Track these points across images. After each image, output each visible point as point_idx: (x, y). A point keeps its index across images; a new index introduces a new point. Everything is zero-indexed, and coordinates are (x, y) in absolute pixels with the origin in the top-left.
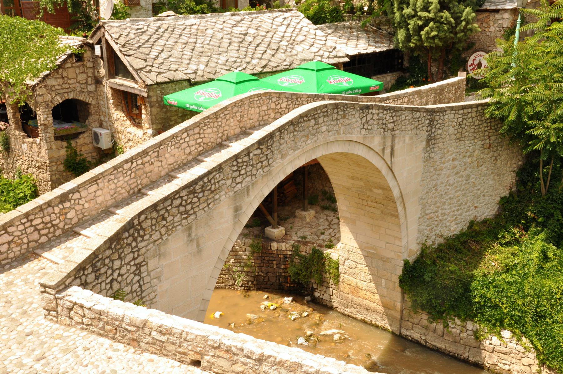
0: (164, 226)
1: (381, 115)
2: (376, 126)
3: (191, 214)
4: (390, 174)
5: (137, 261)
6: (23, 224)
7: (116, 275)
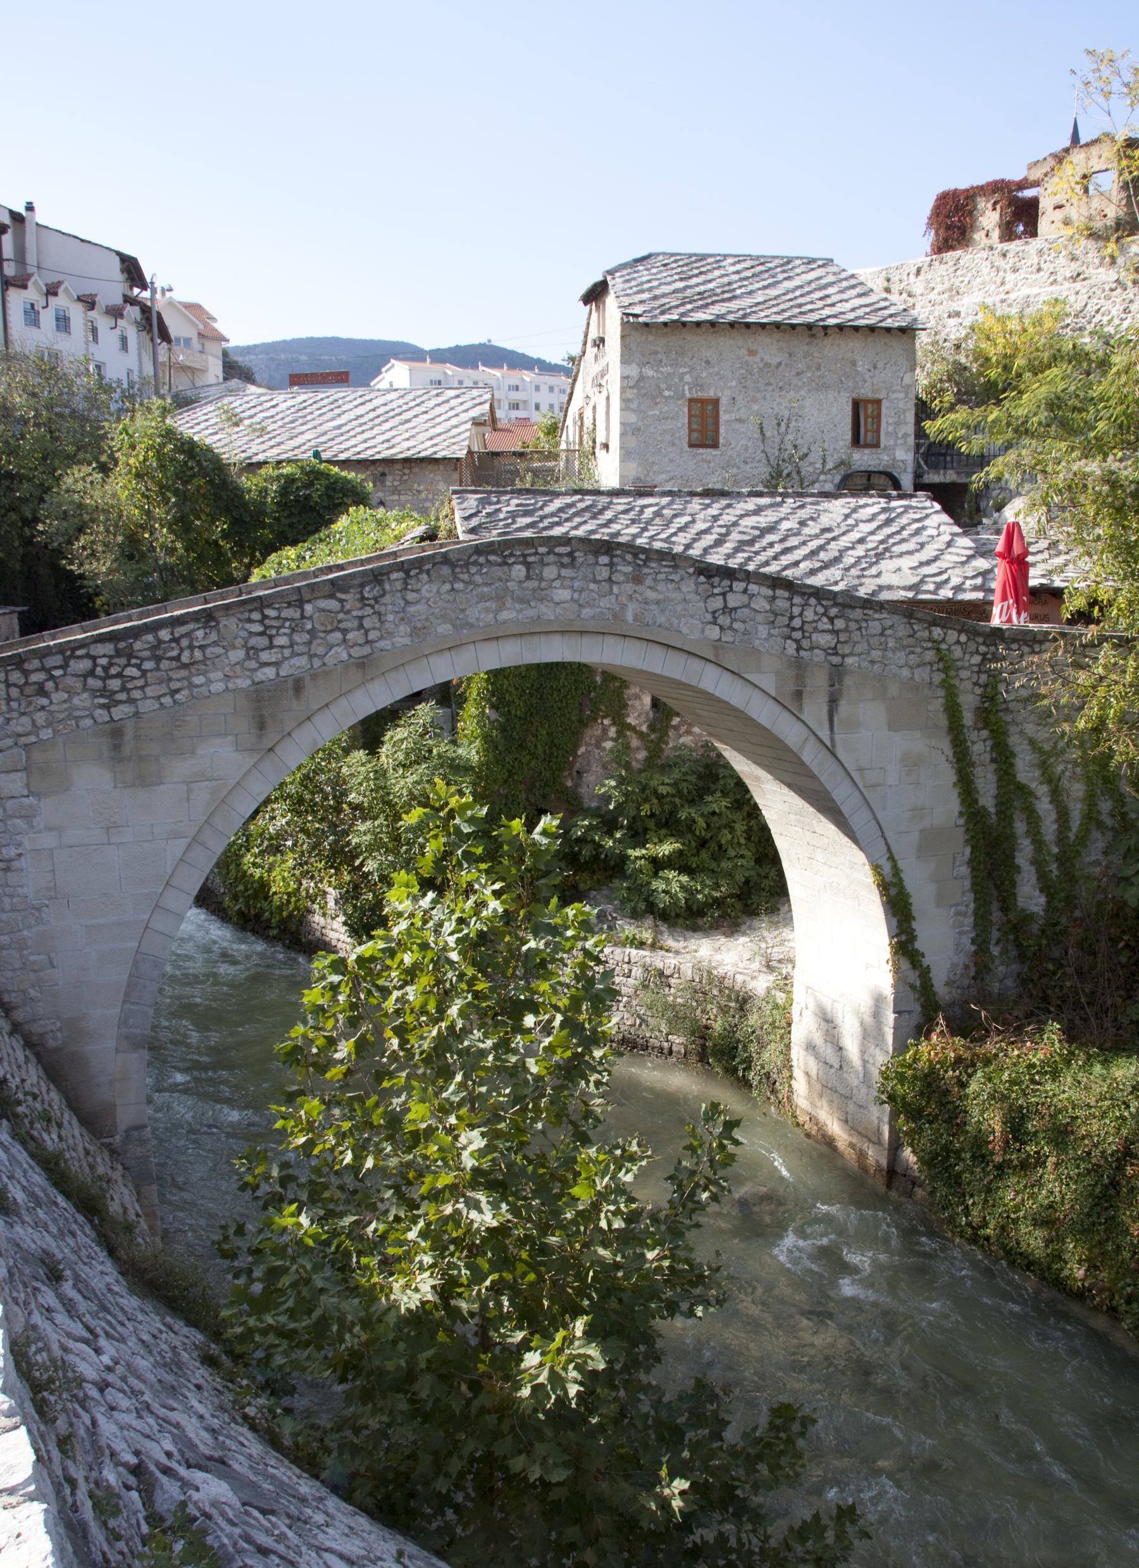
0: (43, 708)
1: (782, 604)
2: (763, 631)
3: (121, 702)
4: (831, 765)
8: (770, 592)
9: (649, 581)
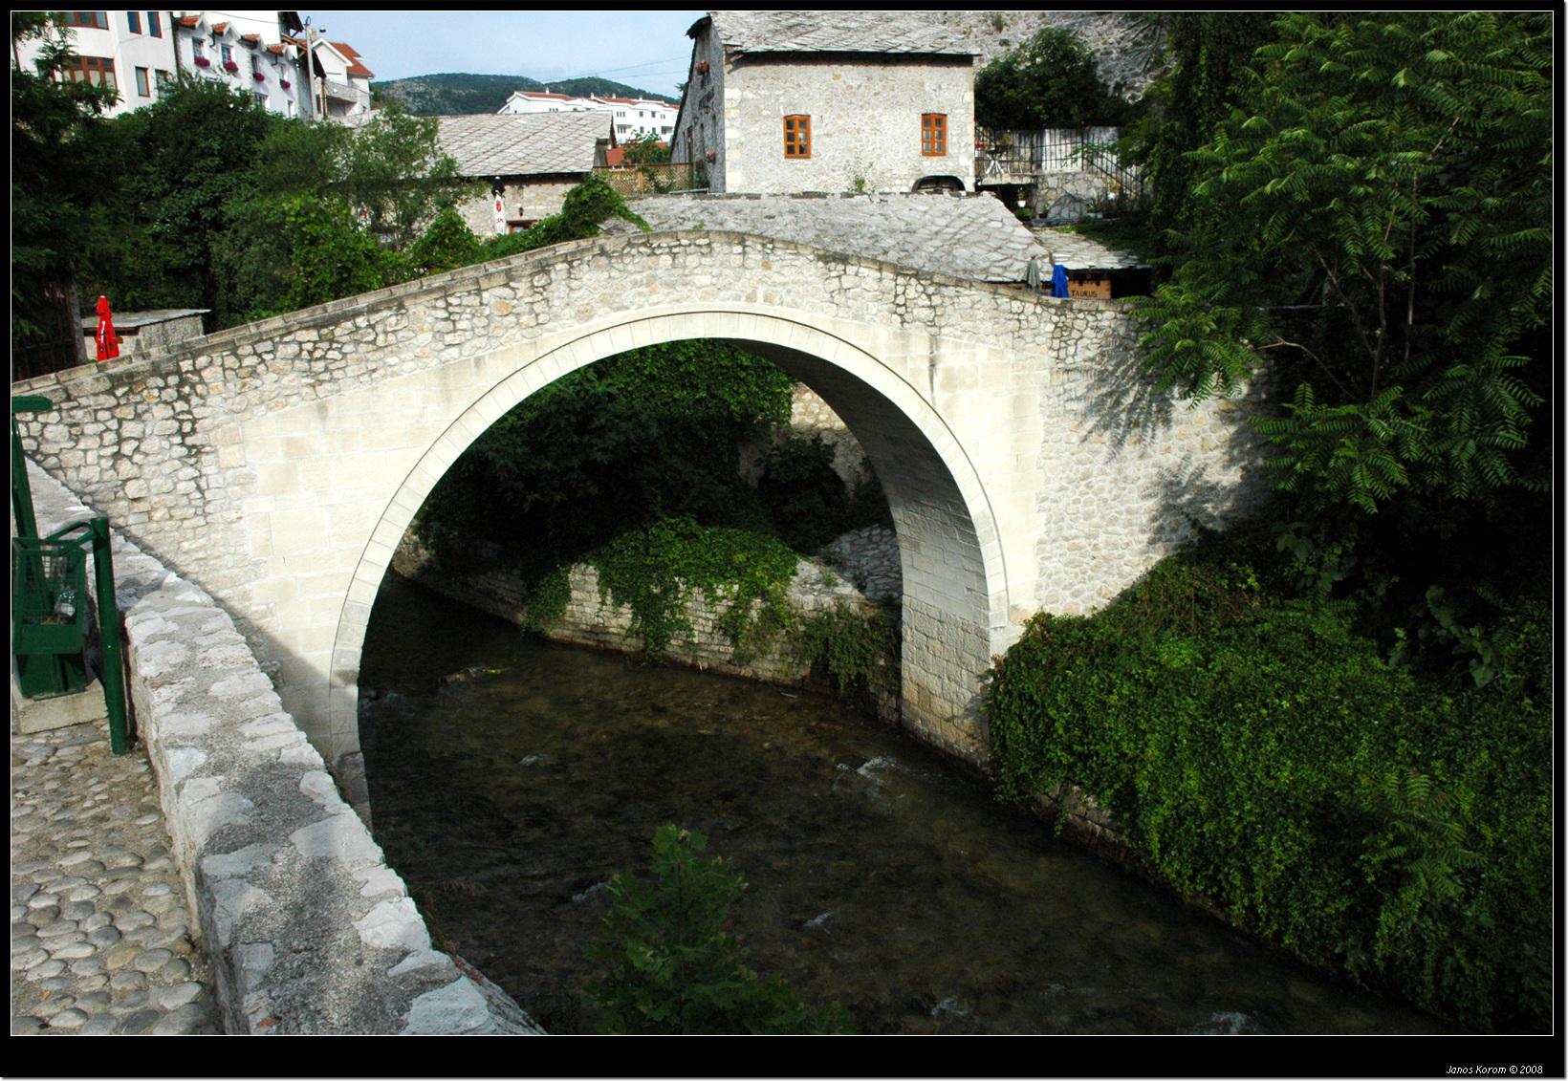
5: (189, 441)
7: (127, 448)
8: (878, 274)
9: (776, 267)
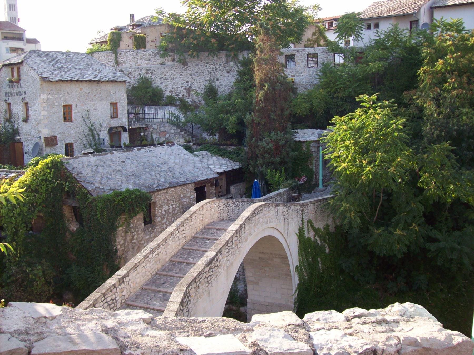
6: (103, 301)
